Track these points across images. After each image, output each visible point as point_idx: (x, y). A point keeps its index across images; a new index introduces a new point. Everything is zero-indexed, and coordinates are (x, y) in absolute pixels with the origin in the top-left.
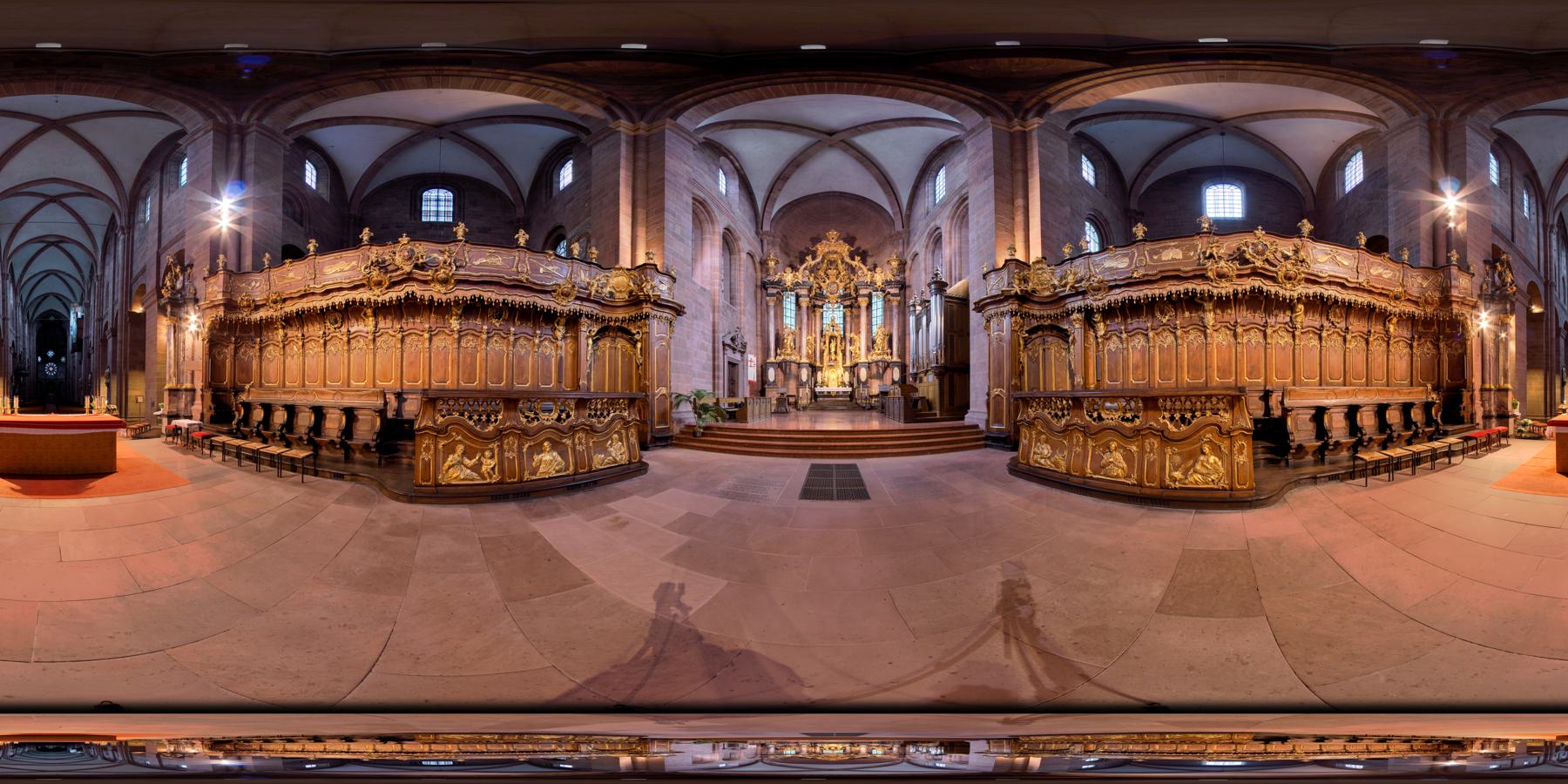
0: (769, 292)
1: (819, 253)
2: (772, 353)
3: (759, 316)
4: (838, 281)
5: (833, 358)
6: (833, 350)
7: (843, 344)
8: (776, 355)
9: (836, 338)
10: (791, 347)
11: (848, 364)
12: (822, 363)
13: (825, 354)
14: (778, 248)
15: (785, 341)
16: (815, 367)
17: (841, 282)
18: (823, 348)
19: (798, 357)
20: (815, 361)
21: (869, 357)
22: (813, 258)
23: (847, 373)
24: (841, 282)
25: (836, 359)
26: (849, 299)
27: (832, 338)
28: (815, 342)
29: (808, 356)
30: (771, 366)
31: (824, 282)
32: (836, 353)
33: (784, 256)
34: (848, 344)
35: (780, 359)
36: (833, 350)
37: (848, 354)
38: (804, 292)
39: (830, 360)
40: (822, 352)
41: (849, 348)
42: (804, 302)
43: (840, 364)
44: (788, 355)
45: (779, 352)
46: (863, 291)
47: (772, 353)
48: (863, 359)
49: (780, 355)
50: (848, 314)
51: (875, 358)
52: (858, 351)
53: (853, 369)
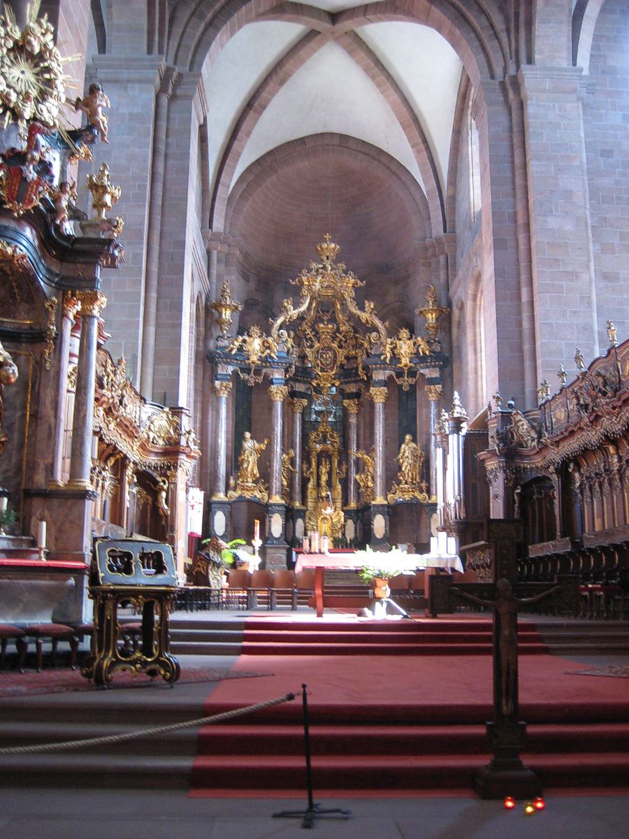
1: (305, 291)
2: (222, 485)
3: (199, 415)
4: (335, 345)
6: (324, 478)
7: (344, 468)
8: (228, 487)
11: (353, 505)
12: (304, 501)
13: (310, 485)
15: (245, 465)
17: (340, 347)
19: (266, 494)
21: (390, 496)
22: (296, 306)
23: (350, 522)
24: (340, 347)
26: (355, 382)
31: (311, 347)
32: (330, 484)
34: (353, 469)
35: (234, 495)
36: (324, 478)
38: (278, 375)
39: (319, 498)
40: (305, 482)
41: (354, 476)
43: (339, 504)
45: (232, 482)
46: (380, 376)
47: (222, 485)
48: (379, 500)
49: (235, 489)
50: (353, 410)
51: (398, 497)
52: (370, 484)
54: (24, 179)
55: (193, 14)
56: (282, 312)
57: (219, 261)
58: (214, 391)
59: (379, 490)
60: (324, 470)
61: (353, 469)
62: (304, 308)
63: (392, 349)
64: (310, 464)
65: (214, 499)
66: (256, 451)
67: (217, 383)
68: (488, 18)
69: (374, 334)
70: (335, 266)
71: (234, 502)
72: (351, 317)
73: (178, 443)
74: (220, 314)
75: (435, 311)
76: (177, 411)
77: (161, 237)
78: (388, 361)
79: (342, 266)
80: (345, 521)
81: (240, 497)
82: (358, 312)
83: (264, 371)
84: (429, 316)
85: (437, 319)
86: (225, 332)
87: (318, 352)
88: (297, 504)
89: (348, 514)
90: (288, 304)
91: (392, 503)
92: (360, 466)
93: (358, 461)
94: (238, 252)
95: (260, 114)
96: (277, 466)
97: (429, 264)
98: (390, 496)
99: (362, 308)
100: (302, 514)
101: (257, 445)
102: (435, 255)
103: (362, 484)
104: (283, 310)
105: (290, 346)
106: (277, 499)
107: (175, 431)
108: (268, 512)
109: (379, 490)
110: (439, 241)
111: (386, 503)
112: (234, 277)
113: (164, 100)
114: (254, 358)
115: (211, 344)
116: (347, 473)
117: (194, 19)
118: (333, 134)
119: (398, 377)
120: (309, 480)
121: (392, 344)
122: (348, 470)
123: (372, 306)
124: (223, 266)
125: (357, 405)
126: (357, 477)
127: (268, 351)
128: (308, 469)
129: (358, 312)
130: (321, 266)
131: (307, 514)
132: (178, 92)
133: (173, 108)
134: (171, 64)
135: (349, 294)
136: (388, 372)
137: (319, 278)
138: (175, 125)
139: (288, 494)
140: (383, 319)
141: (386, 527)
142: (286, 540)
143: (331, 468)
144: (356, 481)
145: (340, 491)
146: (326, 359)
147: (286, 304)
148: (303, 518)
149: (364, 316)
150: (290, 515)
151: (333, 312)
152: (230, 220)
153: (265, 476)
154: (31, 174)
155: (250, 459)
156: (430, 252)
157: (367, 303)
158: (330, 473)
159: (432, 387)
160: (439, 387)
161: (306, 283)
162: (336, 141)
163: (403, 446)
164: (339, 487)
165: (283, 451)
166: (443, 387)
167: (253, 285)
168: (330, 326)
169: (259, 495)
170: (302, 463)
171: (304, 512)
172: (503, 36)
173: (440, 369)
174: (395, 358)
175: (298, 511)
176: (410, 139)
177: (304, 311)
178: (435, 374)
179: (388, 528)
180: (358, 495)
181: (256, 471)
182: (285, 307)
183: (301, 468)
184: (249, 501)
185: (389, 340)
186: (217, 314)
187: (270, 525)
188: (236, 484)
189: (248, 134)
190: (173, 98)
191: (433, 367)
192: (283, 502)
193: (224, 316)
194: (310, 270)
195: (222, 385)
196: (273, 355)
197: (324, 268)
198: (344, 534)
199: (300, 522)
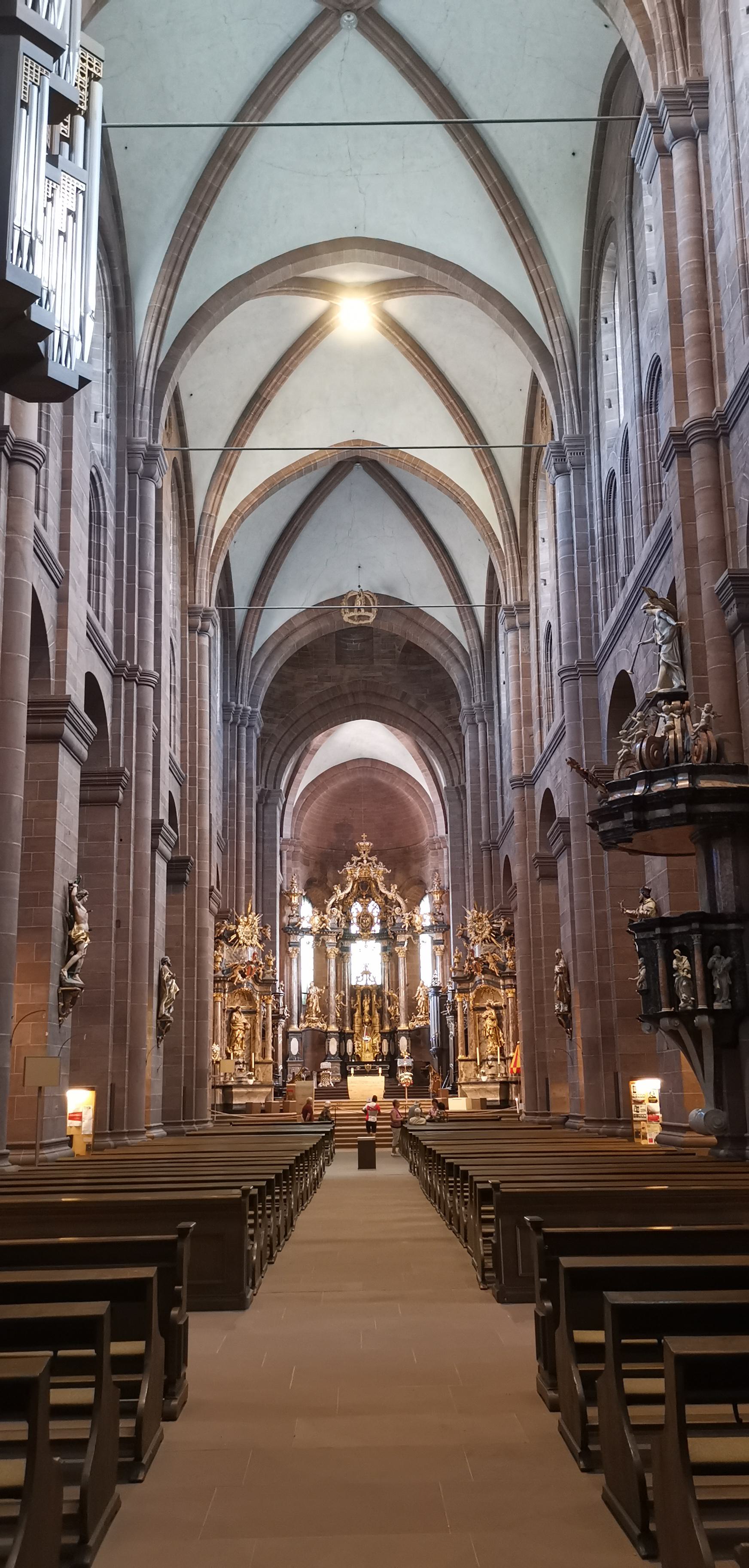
0: (292, 941)
1: (349, 878)
2: (295, 1019)
5: (367, 1020)
6: (367, 1008)
7: (380, 1000)
9: (371, 992)
10: (316, 1012)
11: (387, 1028)
12: (352, 1028)
13: (356, 1015)
14: (299, 862)
15: (311, 1005)
16: (344, 1033)
18: (354, 1007)
19: (325, 1025)
20: (344, 1025)
21: (410, 1023)
22: (342, 890)
23: (385, 1042)
25: (370, 1022)
26: (386, 939)
27: (366, 991)
28: (345, 1003)
29: (337, 1023)
30: (294, 1036)
33: (304, 867)
34: (387, 1002)
35: (304, 1026)
36: (367, 1008)
37: (386, 1015)
39: (363, 1023)
40: (353, 1012)
42: (332, 951)
43: (377, 1029)
44: (314, 1022)
45: (302, 1017)
46: (401, 938)
47: (295, 1019)
48: (403, 1026)
49: (304, 1021)
51: (417, 1024)
52: (397, 1014)
53: (392, 1036)
54: (252, 969)
55: (274, 751)
56: (333, 895)
57: (288, 858)
58: (288, 952)
59: (402, 1018)
60: (366, 1003)
61: (387, 1002)
62: (348, 890)
63: (410, 921)
64: (356, 999)
65: (290, 1030)
66: (319, 995)
67: (290, 949)
68: (449, 744)
69: (398, 908)
70: (369, 858)
71: (304, 1031)
72: (381, 893)
73: (278, 1013)
74: (291, 899)
75: (439, 892)
76: (277, 996)
77: (263, 891)
78: (406, 929)
79: (374, 859)
80: (382, 1040)
81: (308, 1027)
82: (387, 892)
83: (322, 937)
84: (435, 896)
85: (441, 898)
86: (294, 912)
87: (359, 918)
88: (348, 1029)
89: (383, 1035)
90: (337, 888)
91: (411, 1028)
92: (392, 1001)
93: (389, 997)
94: (301, 850)
95: (314, 754)
96: (333, 1004)
97: (437, 854)
98: (410, 1023)
99: (389, 890)
100: (351, 1036)
101: (318, 990)
102: (440, 848)
103: (392, 1014)
104: (331, 893)
105: (339, 916)
106: (333, 1028)
107: (277, 1006)
108: (327, 1037)
109: (402, 1018)
110: (442, 838)
111: (407, 1028)
112: (299, 869)
113: (261, 806)
114: (315, 930)
115: (285, 919)
116: (382, 1004)
117: (275, 753)
118: (366, 759)
119: (414, 939)
120: (355, 1012)
121: (409, 916)
122: (384, 1001)
123: (396, 888)
124: (291, 861)
125: (389, 956)
126: (389, 1009)
127: (324, 924)
128: (355, 1002)
129: (387, 892)
130: (359, 858)
131: (355, 1036)
132: (268, 801)
133: (266, 811)
134: (264, 787)
135: (380, 880)
136: (407, 936)
137: (359, 869)
138: (267, 822)
139: (340, 1023)
140: (404, 898)
141: (408, 1045)
142: (340, 1056)
143: (371, 1001)
144: (388, 1011)
145: (378, 1018)
146: (365, 924)
147: (335, 889)
148: (352, 1038)
149: (390, 895)
150: (343, 1037)
151: (370, 888)
152: (296, 827)
153: (324, 1013)
154: (253, 966)
155: (314, 1001)
156: (436, 846)
157: (392, 887)
158: (370, 1005)
159: (438, 946)
160: (442, 947)
161: (349, 872)
162: (369, 764)
163: (419, 988)
164: (377, 1015)
165: (337, 992)
166: (445, 947)
167: (312, 866)
168: (367, 900)
169: (320, 1025)
170: (350, 998)
171: (353, 1034)
172: (458, 757)
173: (443, 933)
174: (412, 927)
175: (348, 1034)
176: (420, 767)
177: (349, 893)
178: (441, 938)
179: (409, 1046)
180: (391, 1023)
181: (318, 1009)
182: (335, 891)
183: (350, 1002)
184: (313, 1030)
185: (407, 914)
186: (288, 898)
187: (328, 1047)
188: (305, 1019)
189: (306, 768)
190: (266, 804)
191: (439, 932)
192: (337, 1030)
193: (293, 901)
194: (352, 863)
195: (293, 950)
196: (327, 927)
197: (362, 861)
198: (381, 1050)
199: (349, 1043)
